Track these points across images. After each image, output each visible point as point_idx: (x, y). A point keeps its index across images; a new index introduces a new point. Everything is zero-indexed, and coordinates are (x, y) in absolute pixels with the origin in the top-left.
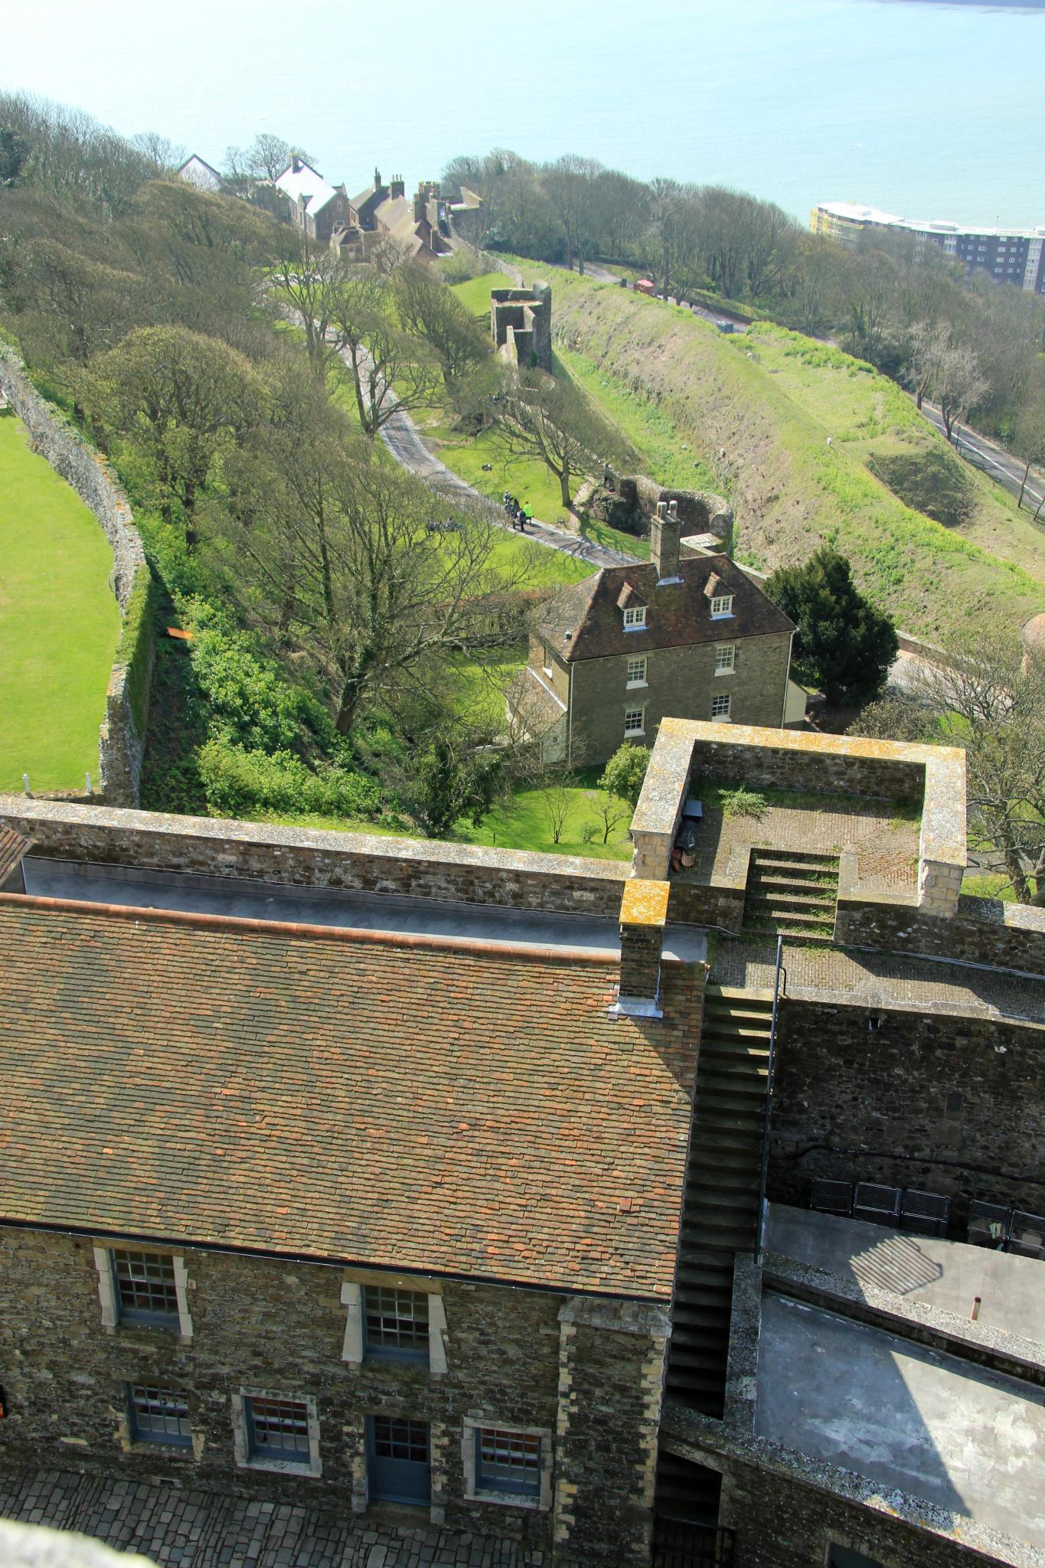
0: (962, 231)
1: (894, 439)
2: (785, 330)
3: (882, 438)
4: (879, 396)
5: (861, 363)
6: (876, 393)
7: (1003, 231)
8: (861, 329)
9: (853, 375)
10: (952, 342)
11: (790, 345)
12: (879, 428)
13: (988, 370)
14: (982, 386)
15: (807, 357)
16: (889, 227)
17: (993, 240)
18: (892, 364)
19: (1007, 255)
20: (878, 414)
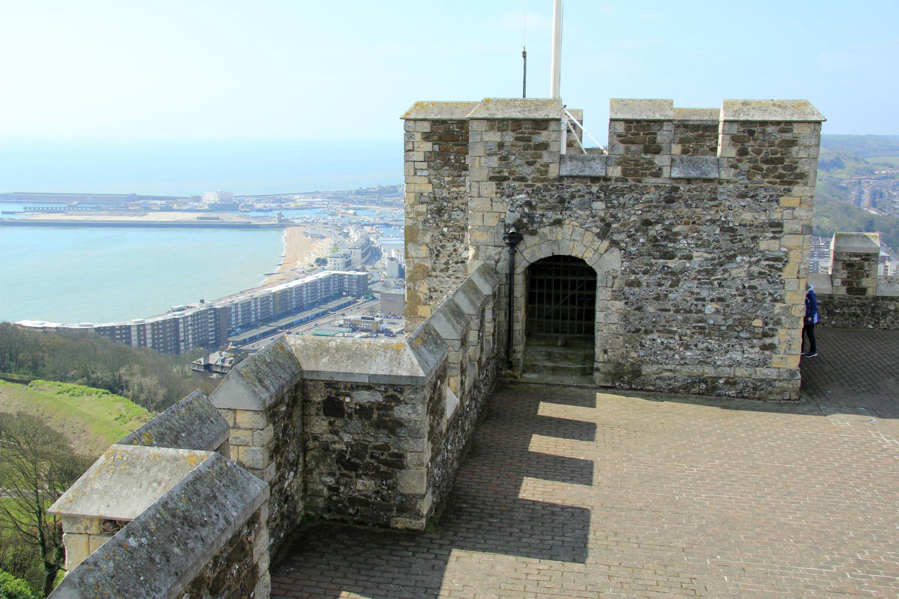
0: (96, 326)
1: (137, 422)
2: (52, 382)
3: (131, 423)
4: (119, 403)
5: (102, 390)
6: (117, 404)
7: (117, 324)
8: (88, 377)
9: (100, 397)
10: (144, 374)
11: (59, 389)
12: (127, 418)
13: (162, 383)
14: (162, 392)
15: (71, 392)
16: (57, 328)
17: (113, 328)
18: (116, 387)
19: (121, 334)
20: (124, 412)
